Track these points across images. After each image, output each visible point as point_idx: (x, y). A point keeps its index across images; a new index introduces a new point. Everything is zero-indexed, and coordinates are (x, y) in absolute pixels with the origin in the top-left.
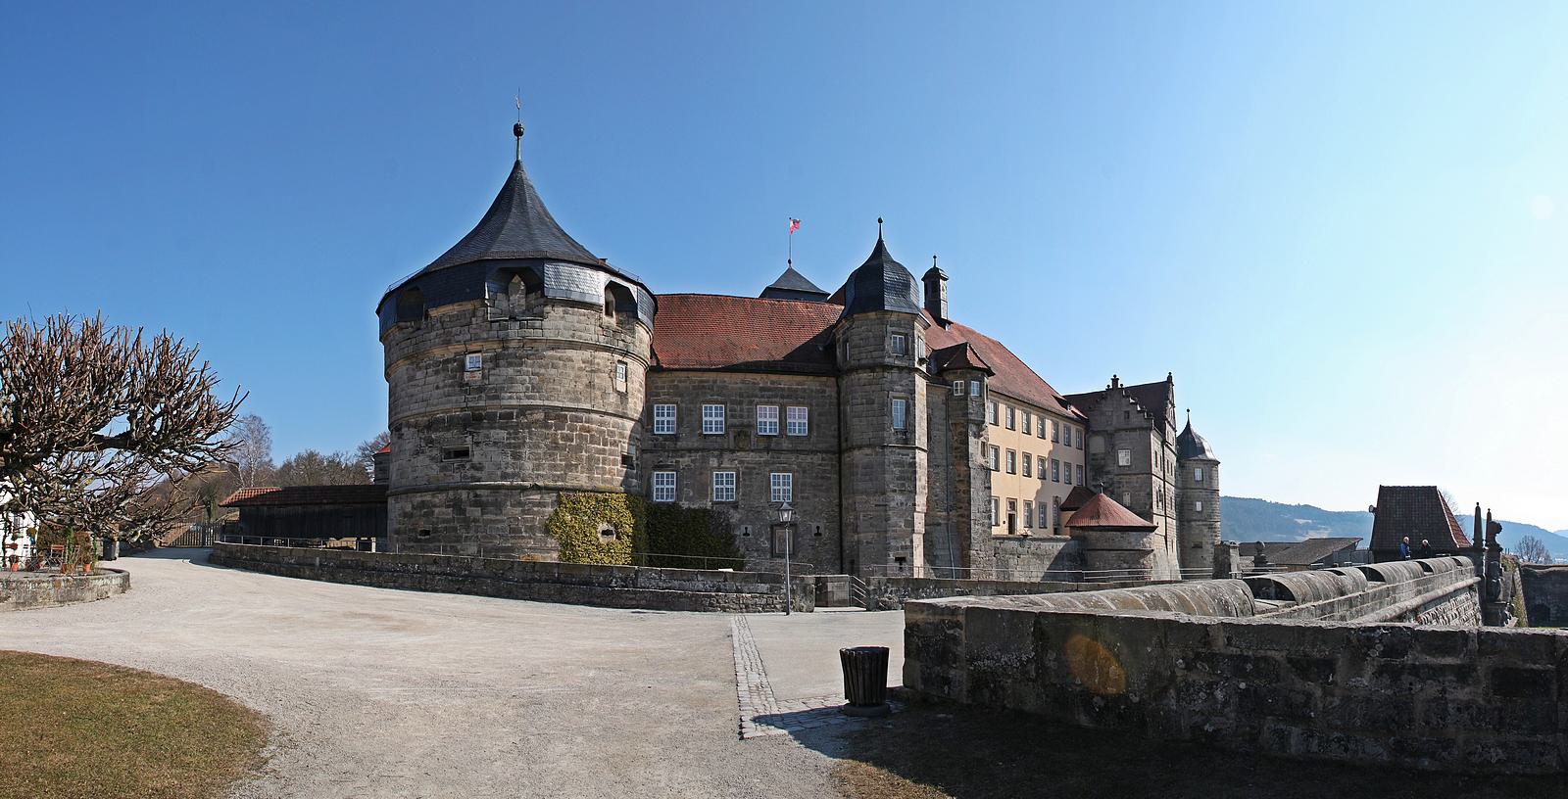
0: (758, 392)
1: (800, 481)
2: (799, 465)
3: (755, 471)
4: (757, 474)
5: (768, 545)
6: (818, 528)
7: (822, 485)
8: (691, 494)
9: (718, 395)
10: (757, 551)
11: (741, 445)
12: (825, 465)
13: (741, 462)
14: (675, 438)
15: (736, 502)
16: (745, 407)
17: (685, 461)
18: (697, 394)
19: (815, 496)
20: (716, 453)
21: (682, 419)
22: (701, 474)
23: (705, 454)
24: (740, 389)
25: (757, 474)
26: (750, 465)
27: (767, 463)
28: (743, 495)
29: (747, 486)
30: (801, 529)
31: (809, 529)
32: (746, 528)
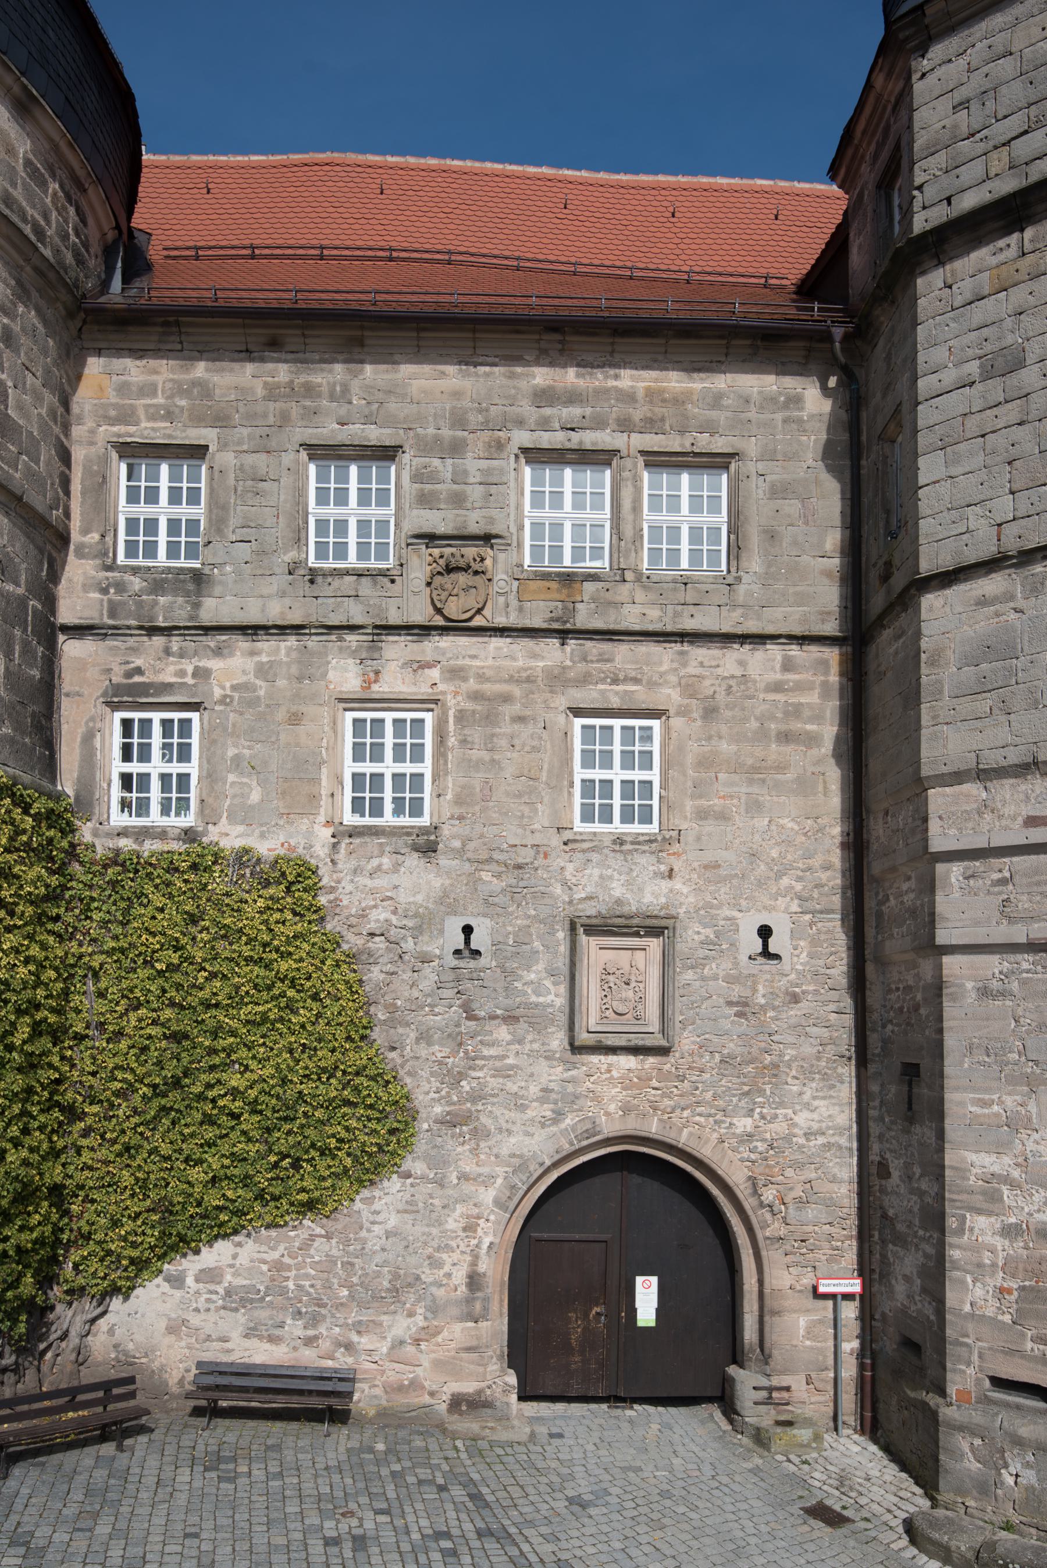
0: (527, 410)
1: (693, 750)
2: (689, 689)
3: (508, 710)
4: (520, 719)
5: (555, 997)
6: (765, 932)
7: (781, 768)
8: (255, 797)
9: (369, 420)
10: (510, 1019)
11: (454, 609)
12: (800, 687)
13: (455, 674)
14: (198, 581)
15: (424, 831)
16: (473, 465)
17: (233, 666)
18: (285, 418)
19: (754, 807)
20: (352, 638)
21: (224, 508)
22: (295, 719)
23: (313, 643)
24: (457, 394)
25: (520, 719)
26: (488, 688)
27: (557, 679)
28: (458, 801)
29: (477, 765)
30: (692, 935)
31: (721, 941)
32: (468, 930)
